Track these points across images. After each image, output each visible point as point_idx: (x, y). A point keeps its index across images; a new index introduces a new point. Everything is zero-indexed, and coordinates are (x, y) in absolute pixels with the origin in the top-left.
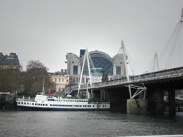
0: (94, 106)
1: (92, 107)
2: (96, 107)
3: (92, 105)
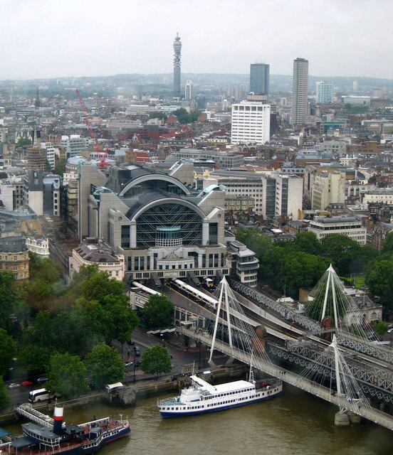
0: (263, 394)
1: (261, 397)
2: (266, 395)
3: (261, 393)
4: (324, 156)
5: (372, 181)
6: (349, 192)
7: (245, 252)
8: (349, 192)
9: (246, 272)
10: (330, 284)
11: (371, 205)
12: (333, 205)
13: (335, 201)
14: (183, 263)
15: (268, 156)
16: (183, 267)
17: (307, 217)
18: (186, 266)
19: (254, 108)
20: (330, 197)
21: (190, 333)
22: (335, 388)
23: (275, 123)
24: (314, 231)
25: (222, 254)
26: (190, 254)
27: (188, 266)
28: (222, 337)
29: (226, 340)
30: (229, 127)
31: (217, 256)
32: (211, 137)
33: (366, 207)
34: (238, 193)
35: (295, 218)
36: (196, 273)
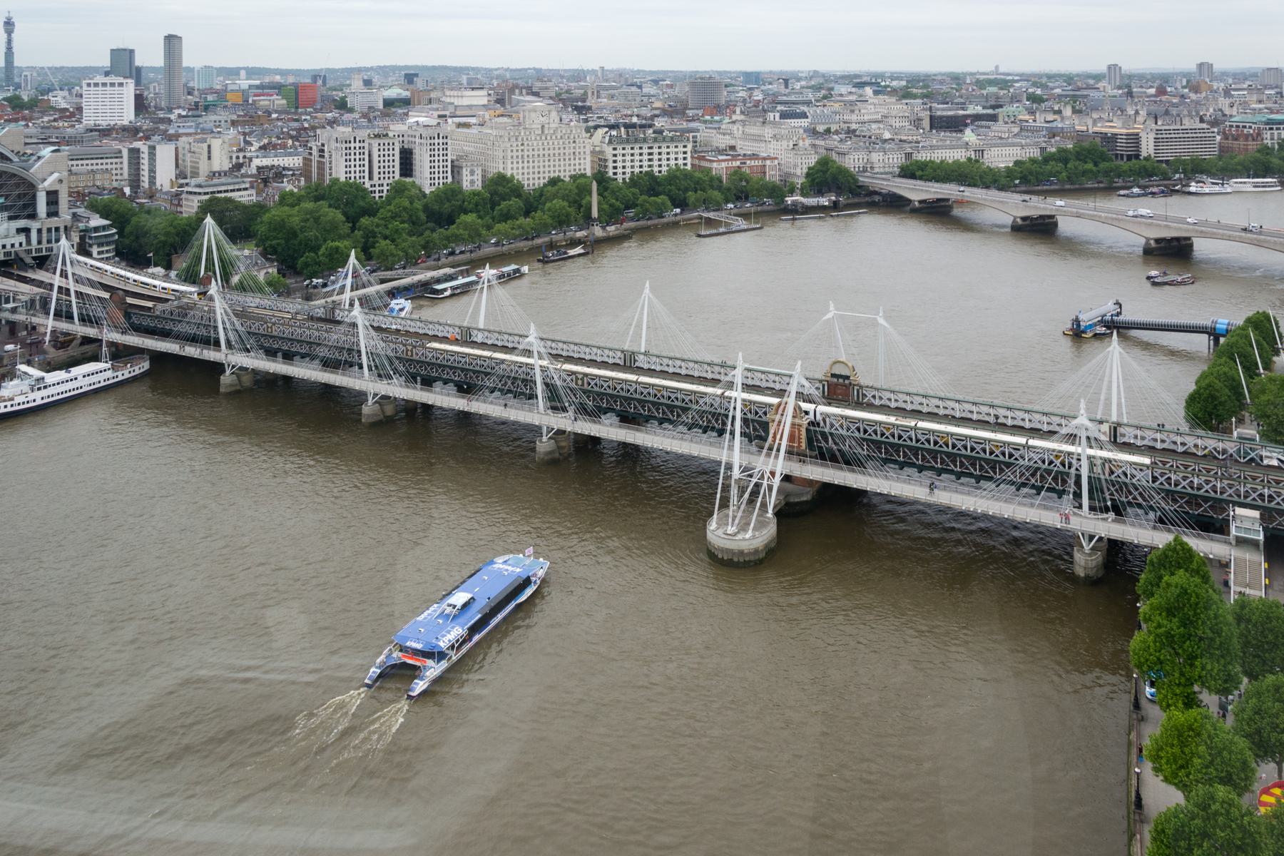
4: (203, 130)
5: (263, 148)
6: (234, 160)
7: (97, 221)
8: (234, 160)
9: (100, 245)
10: (209, 241)
11: (259, 168)
12: (214, 173)
13: (216, 168)
14: (8, 242)
15: (131, 132)
16: (8, 247)
17: (181, 186)
18: (13, 245)
19: (112, 85)
20: (210, 165)
21: (20, 317)
22: (217, 343)
23: (141, 104)
24: (191, 197)
25: (66, 227)
26: (19, 231)
27: (17, 245)
28: (64, 314)
29: (72, 318)
30: (80, 109)
31: (57, 229)
32: (55, 120)
33: (254, 171)
34: (90, 168)
35: (167, 188)
36: (29, 252)
